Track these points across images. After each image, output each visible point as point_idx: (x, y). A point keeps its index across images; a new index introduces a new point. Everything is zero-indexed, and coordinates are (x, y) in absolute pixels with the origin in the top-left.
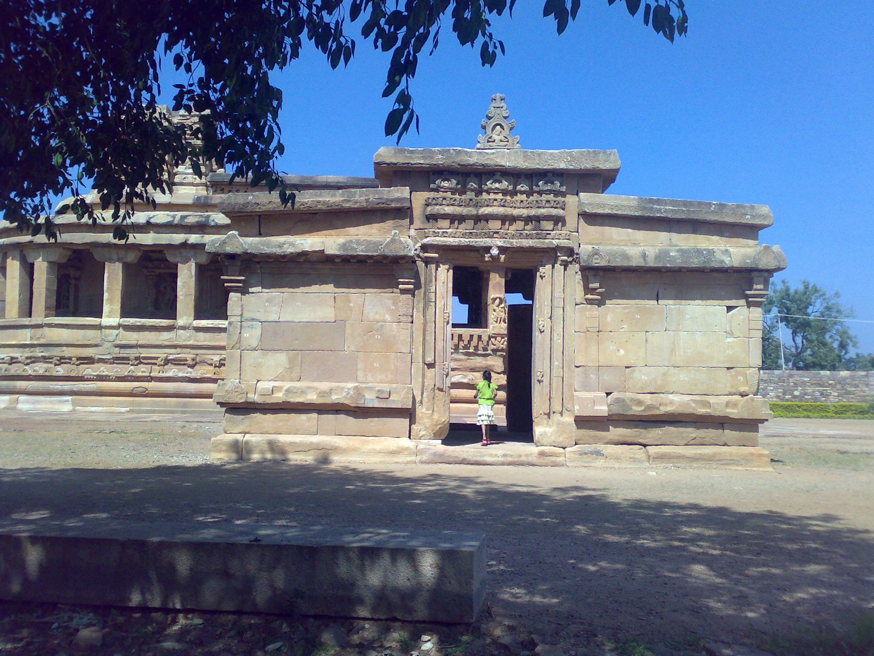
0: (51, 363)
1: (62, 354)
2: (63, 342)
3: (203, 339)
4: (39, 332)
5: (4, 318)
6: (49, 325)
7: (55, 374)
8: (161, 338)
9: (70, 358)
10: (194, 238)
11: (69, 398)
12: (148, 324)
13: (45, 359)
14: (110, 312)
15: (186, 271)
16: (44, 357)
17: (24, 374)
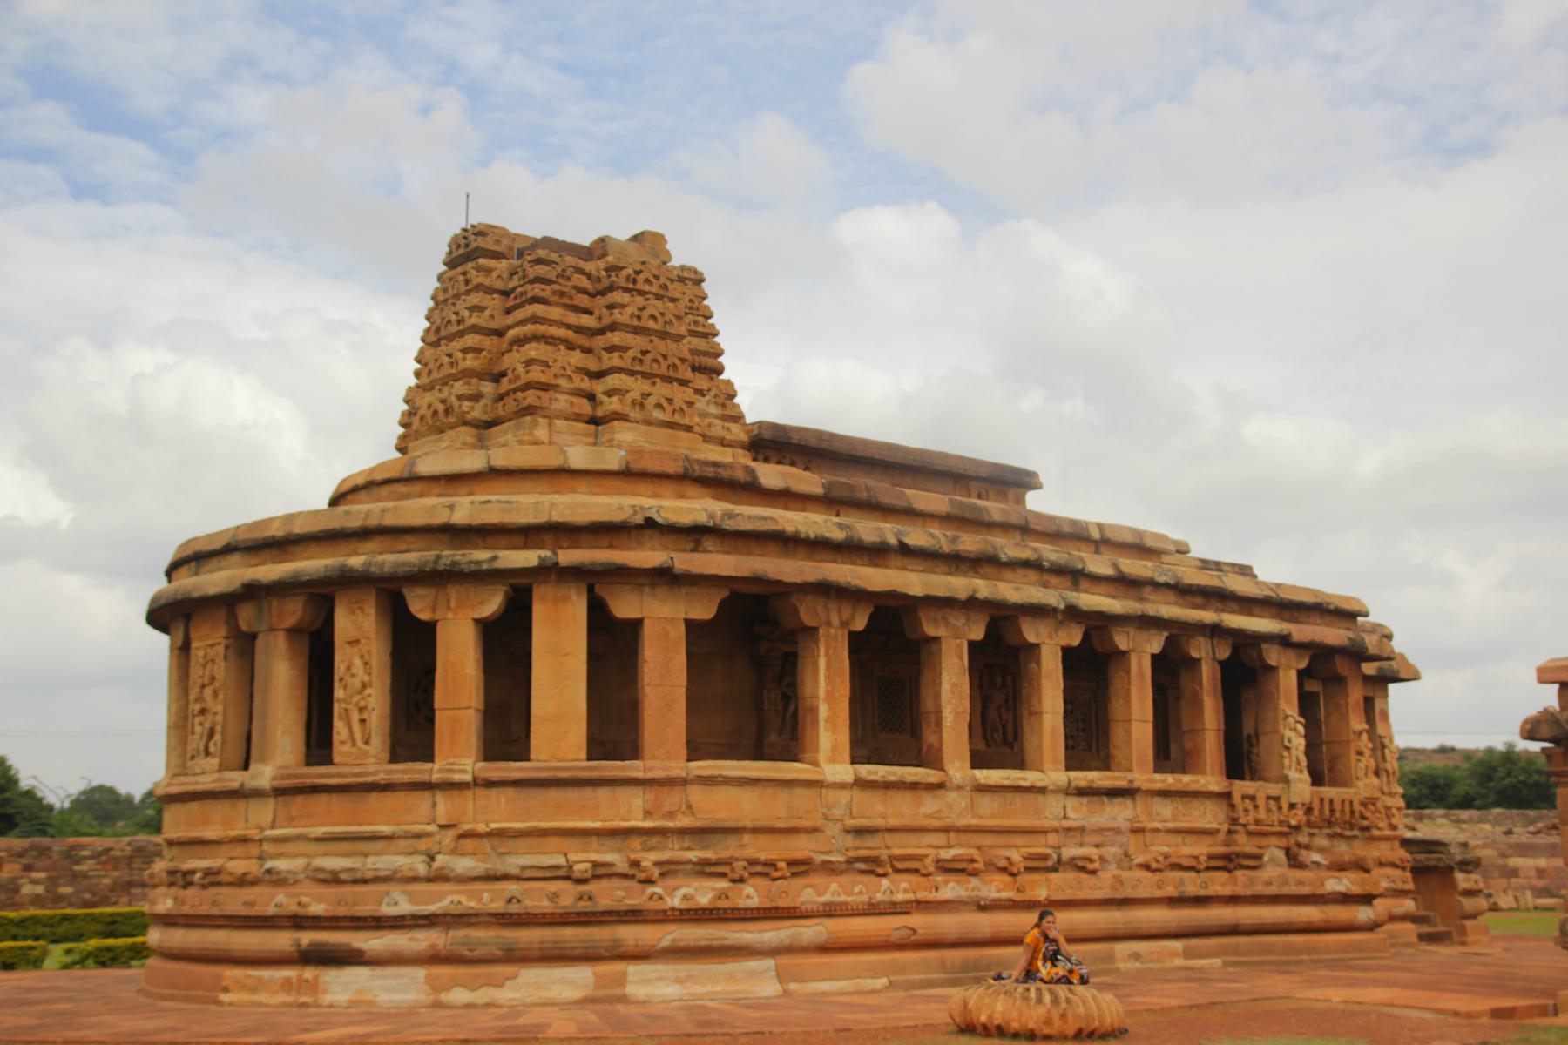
0: (723, 875)
1: (750, 852)
2: (749, 824)
3: (989, 811)
4: (673, 798)
5: (528, 760)
6: (708, 781)
7: (742, 904)
8: (923, 810)
9: (771, 864)
10: (983, 587)
11: (769, 963)
12: (909, 779)
13: (704, 869)
14: (834, 749)
15: (955, 660)
16: (705, 862)
17: (653, 905)
